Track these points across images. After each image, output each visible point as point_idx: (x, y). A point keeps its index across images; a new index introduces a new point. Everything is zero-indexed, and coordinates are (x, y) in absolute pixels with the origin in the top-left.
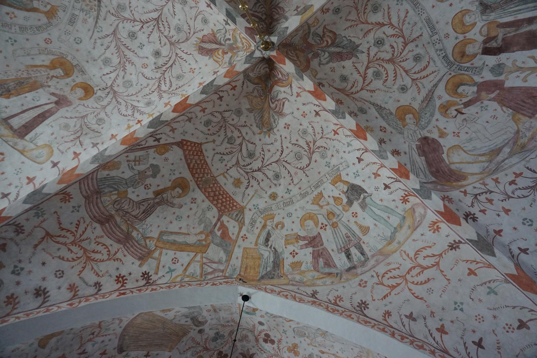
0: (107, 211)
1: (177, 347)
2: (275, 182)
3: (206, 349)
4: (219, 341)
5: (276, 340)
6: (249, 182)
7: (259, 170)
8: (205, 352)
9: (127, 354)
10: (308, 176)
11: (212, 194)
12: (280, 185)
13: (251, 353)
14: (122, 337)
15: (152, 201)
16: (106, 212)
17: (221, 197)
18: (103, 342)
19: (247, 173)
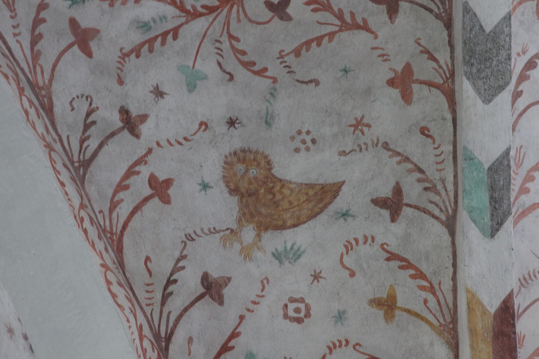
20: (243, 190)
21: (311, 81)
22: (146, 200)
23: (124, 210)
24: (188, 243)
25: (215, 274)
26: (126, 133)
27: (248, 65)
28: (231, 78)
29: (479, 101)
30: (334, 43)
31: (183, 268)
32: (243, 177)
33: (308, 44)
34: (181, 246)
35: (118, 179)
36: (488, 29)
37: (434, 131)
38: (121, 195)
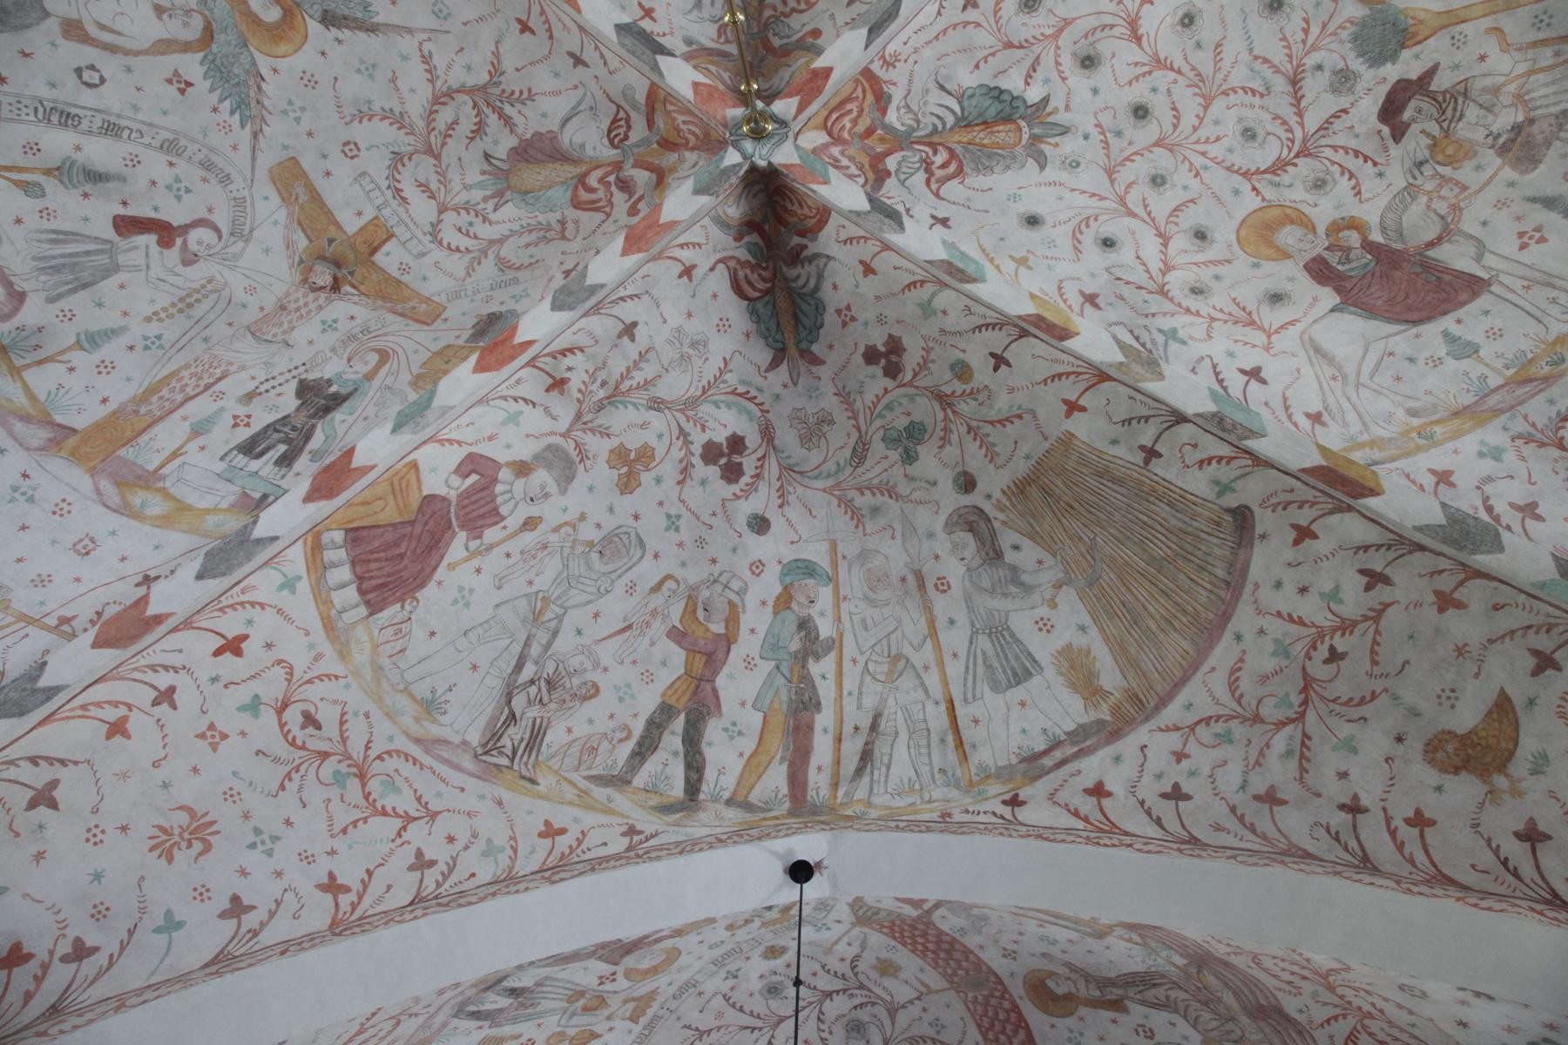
0: (1262, 1031)
1: (1047, 445)
2: (775, 978)
3: (944, 400)
4: (902, 422)
5: (702, 470)
6: (853, 968)
7: (829, 995)
8: (947, 390)
9: (1220, 494)
10: (685, 1026)
11: (957, 955)
12: (761, 976)
13: (784, 367)
14: (1235, 582)
15: (1131, 995)
16: (1267, 1030)
17: (931, 946)
18: (1303, 590)
19: (862, 986)
20: (1460, 764)
21: (1403, 665)
22: (1422, 836)
23: (1420, 857)
24: (1479, 829)
25: (1520, 827)
26: (1359, 817)
27: (1362, 701)
28: (1365, 719)
29: (1499, 556)
30: (1384, 634)
31: (1498, 846)
32: (1449, 758)
33: (1373, 652)
34: (1478, 836)
35: (1391, 845)
36: (1444, 522)
37: (1502, 601)
38: (1407, 851)
